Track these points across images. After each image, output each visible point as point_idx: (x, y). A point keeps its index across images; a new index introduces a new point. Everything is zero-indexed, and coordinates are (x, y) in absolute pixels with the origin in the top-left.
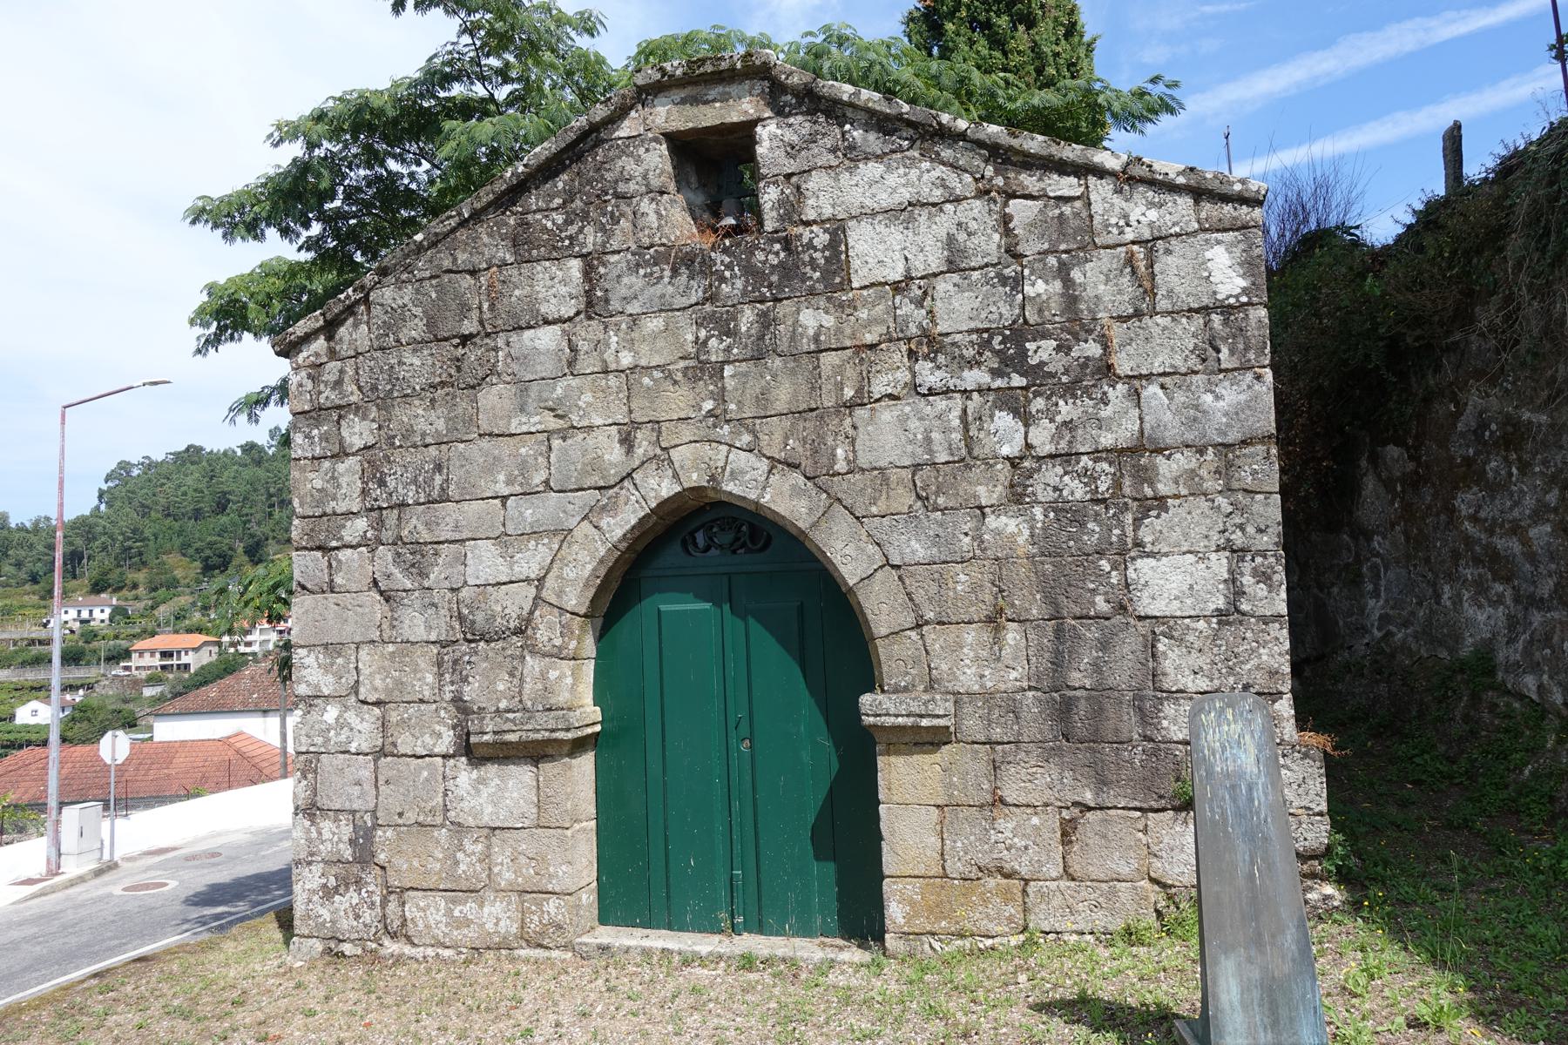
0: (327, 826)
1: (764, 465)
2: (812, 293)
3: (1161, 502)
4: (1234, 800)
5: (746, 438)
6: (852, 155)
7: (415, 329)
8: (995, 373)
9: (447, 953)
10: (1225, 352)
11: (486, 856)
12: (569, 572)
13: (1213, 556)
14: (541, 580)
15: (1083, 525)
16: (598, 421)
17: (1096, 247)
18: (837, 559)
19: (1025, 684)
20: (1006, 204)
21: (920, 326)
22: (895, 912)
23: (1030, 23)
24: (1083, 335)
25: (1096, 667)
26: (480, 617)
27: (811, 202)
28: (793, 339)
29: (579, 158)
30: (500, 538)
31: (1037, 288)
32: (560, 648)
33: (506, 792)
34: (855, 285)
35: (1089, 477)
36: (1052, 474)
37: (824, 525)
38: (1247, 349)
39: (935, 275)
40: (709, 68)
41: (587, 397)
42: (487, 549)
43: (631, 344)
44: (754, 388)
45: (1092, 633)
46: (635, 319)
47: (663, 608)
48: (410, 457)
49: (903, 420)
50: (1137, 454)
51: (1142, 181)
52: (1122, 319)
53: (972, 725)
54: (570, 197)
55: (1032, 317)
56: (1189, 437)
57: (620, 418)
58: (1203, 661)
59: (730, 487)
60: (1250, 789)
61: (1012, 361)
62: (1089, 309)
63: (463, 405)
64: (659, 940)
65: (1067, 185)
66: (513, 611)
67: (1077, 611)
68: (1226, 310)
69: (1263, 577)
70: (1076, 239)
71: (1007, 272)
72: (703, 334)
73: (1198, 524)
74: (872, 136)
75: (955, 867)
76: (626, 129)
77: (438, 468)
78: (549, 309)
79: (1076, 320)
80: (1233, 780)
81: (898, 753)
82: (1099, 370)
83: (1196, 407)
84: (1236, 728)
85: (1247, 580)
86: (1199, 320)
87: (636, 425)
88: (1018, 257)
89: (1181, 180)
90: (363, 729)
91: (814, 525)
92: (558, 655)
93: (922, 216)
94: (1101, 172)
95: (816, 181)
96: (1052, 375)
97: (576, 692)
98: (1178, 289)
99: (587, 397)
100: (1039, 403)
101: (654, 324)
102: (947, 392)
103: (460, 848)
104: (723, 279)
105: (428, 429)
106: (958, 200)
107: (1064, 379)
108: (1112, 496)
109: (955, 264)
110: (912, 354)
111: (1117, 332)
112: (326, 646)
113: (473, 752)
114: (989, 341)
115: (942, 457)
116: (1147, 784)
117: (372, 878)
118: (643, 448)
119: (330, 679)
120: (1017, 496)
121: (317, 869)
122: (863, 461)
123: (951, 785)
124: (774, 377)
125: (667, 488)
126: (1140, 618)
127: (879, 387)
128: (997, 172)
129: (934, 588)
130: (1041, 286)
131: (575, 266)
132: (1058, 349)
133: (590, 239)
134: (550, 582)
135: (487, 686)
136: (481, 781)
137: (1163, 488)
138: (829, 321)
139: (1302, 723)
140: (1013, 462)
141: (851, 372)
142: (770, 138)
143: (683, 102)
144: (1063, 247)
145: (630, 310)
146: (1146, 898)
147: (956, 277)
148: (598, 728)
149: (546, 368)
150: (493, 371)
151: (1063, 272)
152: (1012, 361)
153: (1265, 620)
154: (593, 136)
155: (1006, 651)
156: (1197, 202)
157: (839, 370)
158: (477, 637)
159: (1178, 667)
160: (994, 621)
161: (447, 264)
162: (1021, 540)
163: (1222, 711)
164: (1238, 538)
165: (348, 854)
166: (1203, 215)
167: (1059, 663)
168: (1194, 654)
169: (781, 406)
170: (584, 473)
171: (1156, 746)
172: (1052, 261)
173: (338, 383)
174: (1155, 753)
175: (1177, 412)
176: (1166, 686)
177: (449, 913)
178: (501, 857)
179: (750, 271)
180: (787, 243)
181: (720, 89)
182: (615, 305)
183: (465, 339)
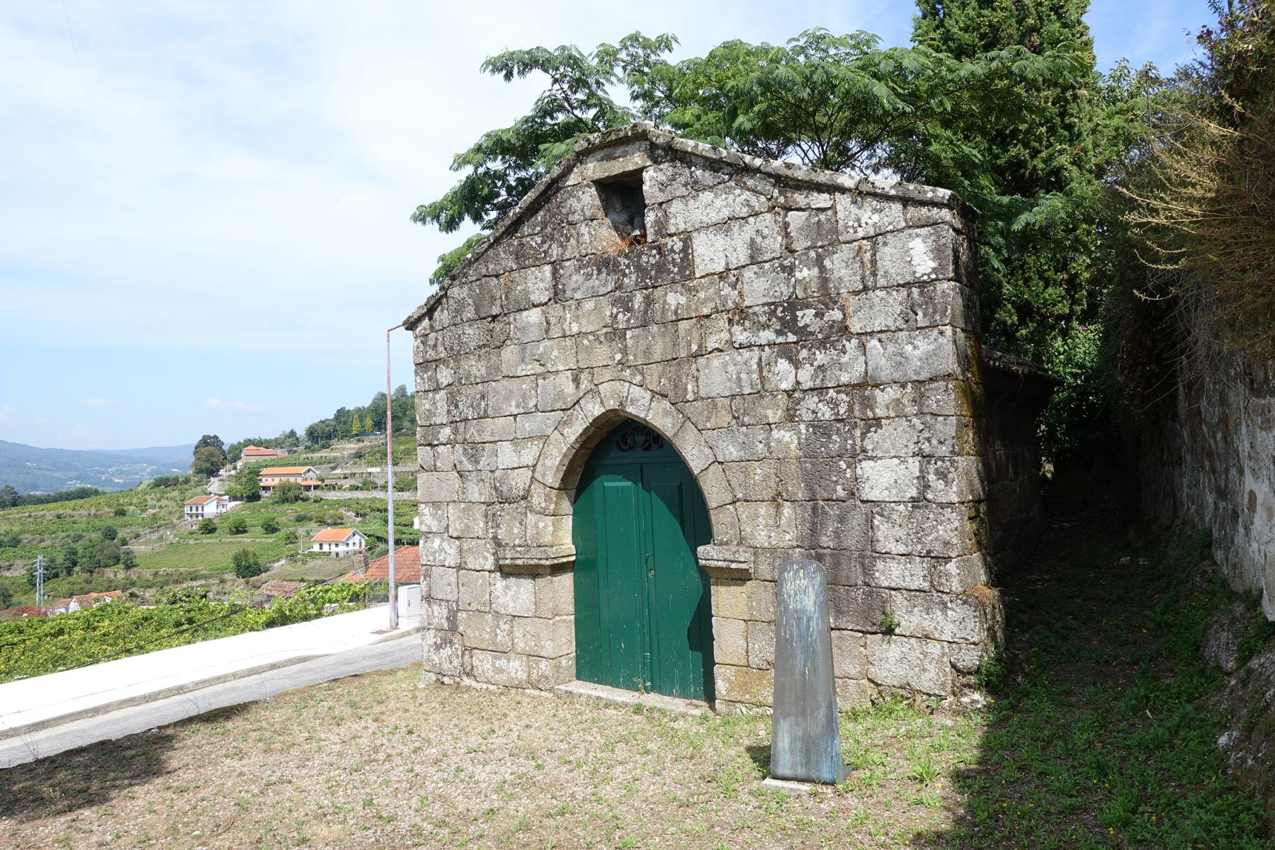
1: (648, 395)
2: (673, 282)
3: (877, 422)
4: (798, 627)
5: (639, 378)
6: (696, 187)
7: (469, 313)
8: (779, 333)
9: (492, 688)
10: (920, 314)
11: (511, 632)
12: (549, 463)
13: (910, 460)
14: (534, 466)
15: (830, 437)
16: (561, 368)
17: (840, 243)
18: (688, 457)
19: (795, 544)
20: (786, 215)
21: (734, 302)
22: (721, 686)
24: (831, 305)
25: (837, 534)
26: (505, 488)
27: (672, 221)
28: (663, 312)
29: (548, 200)
31: (804, 273)
32: (545, 509)
33: (516, 595)
34: (697, 275)
35: (834, 404)
36: (811, 401)
37: (681, 435)
38: (934, 313)
39: (743, 267)
40: (613, 137)
41: (555, 353)
42: (506, 447)
43: (577, 318)
44: (642, 347)
45: (834, 511)
46: (579, 302)
47: (606, 484)
49: (725, 365)
50: (865, 386)
51: (868, 194)
52: (856, 293)
53: (764, 569)
54: (544, 225)
55: (800, 294)
56: (896, 376)
57: (573, 366)
58: (901, 533)
59: (630, 410)
60: (808, 621)
61: (790, 325)
62: (836, 288)
64: (604, 692)
65: (822, 200)
66: (521, 485)
67: (826, 495)
68: (922, 285)
69: (942, 475)
70: (828, 237)
71: (785, 263)
72: (615, 310)
73: (901, 437)
74: (707, 173)
75: (755, 661)
76: (572, 180)
77: (483, 397)
78: (535, 298)
79: (828, 298)
80: (799, 613)
81: (722, 584)
82: (840, 330)
83: (901, 355)
84: (805, 582)
85: (932, 477)
86: (904, 292)
87: (581, 370)
88: (792, 251)
89: (893, 192)
90: (450, 553)
91: (675, 435)
92: (543, 513)
93: (735, 226)
94: (843, 190)
95: (676, 207)
96: (812, 333)
97: (560, 537)
98: (891, 271)
99: (555, 353)
100: (804, 353)
101: (589, 305)
102: (750, 346)
103: (498, 627)
104: (625, 275)
105: (478, 374)
106: (757, 214)
107: (820, 336)
108: (849, 417)
110: (730, 321)
111: (853, 302)
112: (433, 503)
114: (775, 311)
115: (747, 390)
116: (866, 614)
118: (585, 385)
119: (435, 522)
120: (791, 417)
121: (432, 632)
122: (703, 393)
123: (751, 607)
124: (653, 337)
125: (597, 410)
126: (863, 502)
127: (711, 343)
128: (781, 193)
129: (742, 478)
130: (806, 272)
131: (548, 268)
132: (816, 315)
133: (555, 252)
134: (539, 468)
136: (507, 587)
137: (880, 412)
138: (683, 300)
140: (789, 393)
141: (695, 334)
142: (652, 178)
143: (602, 159)
144: (819, 244)
145: (576, 296)
146: (865, 692)
147: (755, 268)
148: (573, 558)
150: (508, 338)
152: (790, 325)
153: (942, 506)
154: (555, 186)
155: (784, 520)
156: (905, 206)
157: (689, 332)
158: (504, 500)
159: (888, 536)
160: (776, 500)
161: (484, 271)
162: (793, 447)
163: (797, 572)
164: (926, 448)
165: (446, 626)
166: (909, 216)
167: (814, 530)
168: (897, 528)
169: (657, 357)
170: (555, 400)
171: (872, 590)
172: (812, 254)
173: (435, 346)
174: (870, 594)
175: (889, 358)
176: (878, 549)
177: (493, 664)
178: (518, 634)
179: (640, 269)
180: (659, 249)
181: (622, 149)
182: (569, 294)
183: (494, 318)
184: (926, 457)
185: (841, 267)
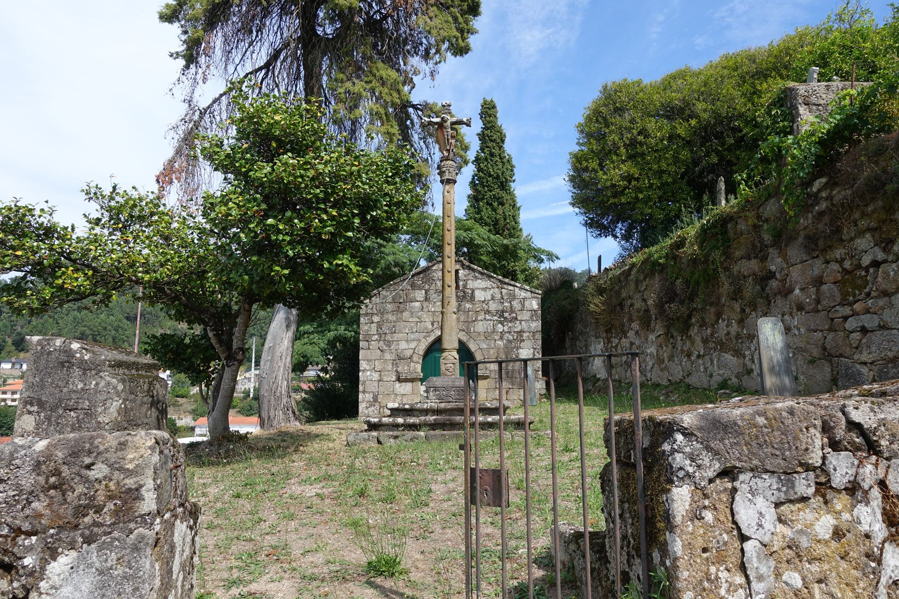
0: (367, 395)
6: (476, 278)
23: (502, 204)
30: (407, 341)
31: (506, 304)
36: (507, 335)
50: (520, 332)
63: (399, 315)
65: (511, 288)
70: (513, 297)
76: (434, 268)
79: (512, 310)
90: (376, 376)
92: (418, 363)
95: (469, 282)
109: (493, 298)
113: (399, 380)
117: (377, 405)
120: (501, 338)
127: (479, 318)
135: (403, 368)
139: (543, 375)
149: (417, 310)
151: (510, 302)
158: (400, 359)
184: (535, 349)
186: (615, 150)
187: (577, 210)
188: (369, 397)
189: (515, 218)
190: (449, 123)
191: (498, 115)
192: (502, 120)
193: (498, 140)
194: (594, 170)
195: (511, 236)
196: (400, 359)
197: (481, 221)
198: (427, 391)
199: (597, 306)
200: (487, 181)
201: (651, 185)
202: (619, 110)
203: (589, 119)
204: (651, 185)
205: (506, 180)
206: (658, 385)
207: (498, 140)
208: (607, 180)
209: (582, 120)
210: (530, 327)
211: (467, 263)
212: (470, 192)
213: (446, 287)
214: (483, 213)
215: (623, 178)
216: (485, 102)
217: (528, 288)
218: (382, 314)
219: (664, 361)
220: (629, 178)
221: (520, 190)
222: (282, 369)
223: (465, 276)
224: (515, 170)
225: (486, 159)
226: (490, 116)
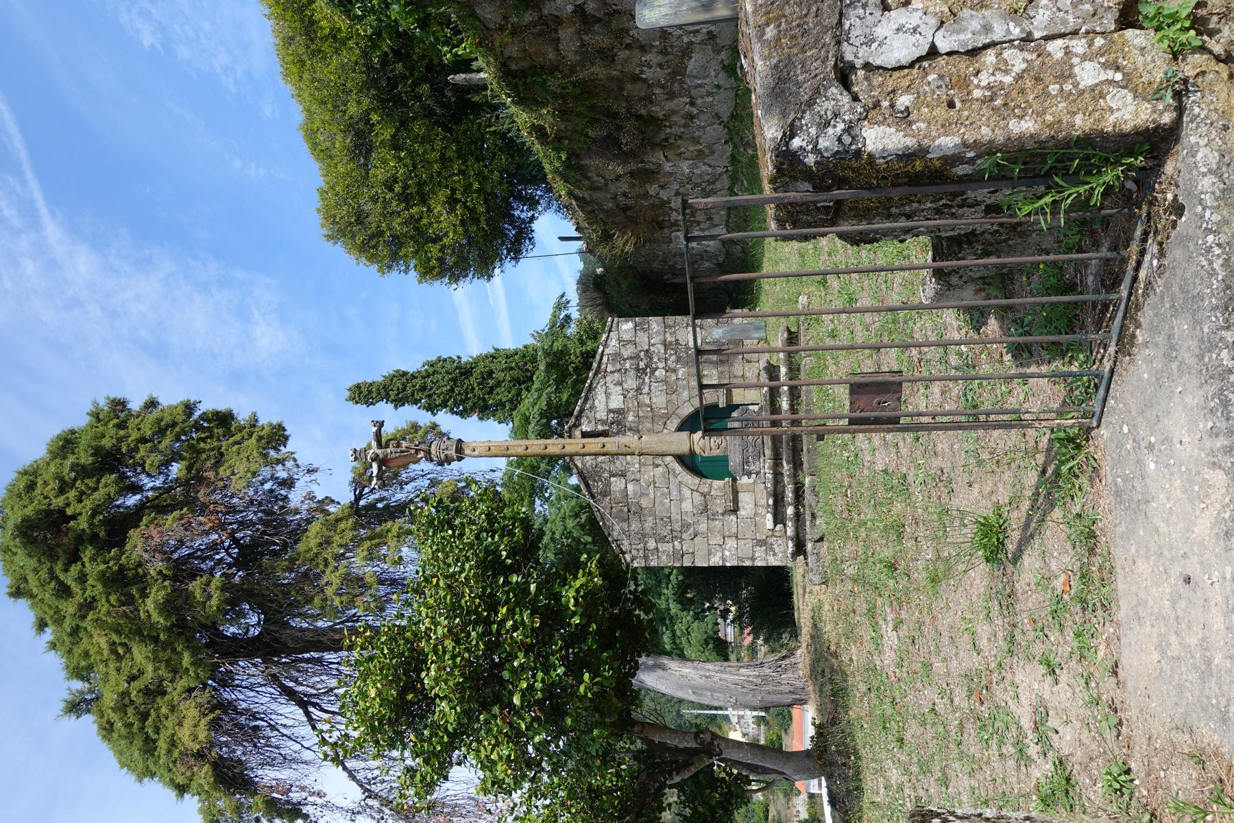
0: (757, 555)
6: (592, 407)
7: (625, 525)
30: (681, 501)
31: (628, 365)
36: (669, 363)
42: (684, 505)
48: (659, 527)
50: (666, 345)
63: (646, 512)
65: (605, 359)
70: (617, 356)
76: (580, 465)
78: (623, 487)
79: (636, 357)
90: (731, 543)
92: (711, 486)
95: (598, 416)
113: (735, 511)
120: (674, 371)
127: (647, 401)
135: (719, 505)
149: (638, 488)
151: (625, 360)
152: (644, 370)
158: (706, 509)
185: (626, 353)
186: (414, 221)
187: (497, 271)
188: (760, 552)
189: (510, 355)
190: (379, 451)
191: (370, 381)
192: (376, 375)
193: (404, 380)
194: (442, 250)
195: (534, 360)
196: (706, 509)
197: (515, 403)
198: (749, 474)
199: (627, 241)
200: (460, 394)
201: (461, 172)
202: (360, 218)
203: (372, 258)
204: (461, 172)
205: (457, 368)
206: (733, 157)
207: (404, 380)
208: (455, 232)
209: (374, 268)
210: (658, 333)
211: (573, 420)
212: (475, 417)
213: (605, 450)
214: (504, 399)
215: (452, 210)
216: (352, 399)
217: (604, 337)
218: (644, 536)
219: (700, 151)
220: (452, 202)
221: (471, 348)
222: (724, 676)
223: (590, 422)
224: (445, 356)
225: (429, 396)
226: (370, 392)
